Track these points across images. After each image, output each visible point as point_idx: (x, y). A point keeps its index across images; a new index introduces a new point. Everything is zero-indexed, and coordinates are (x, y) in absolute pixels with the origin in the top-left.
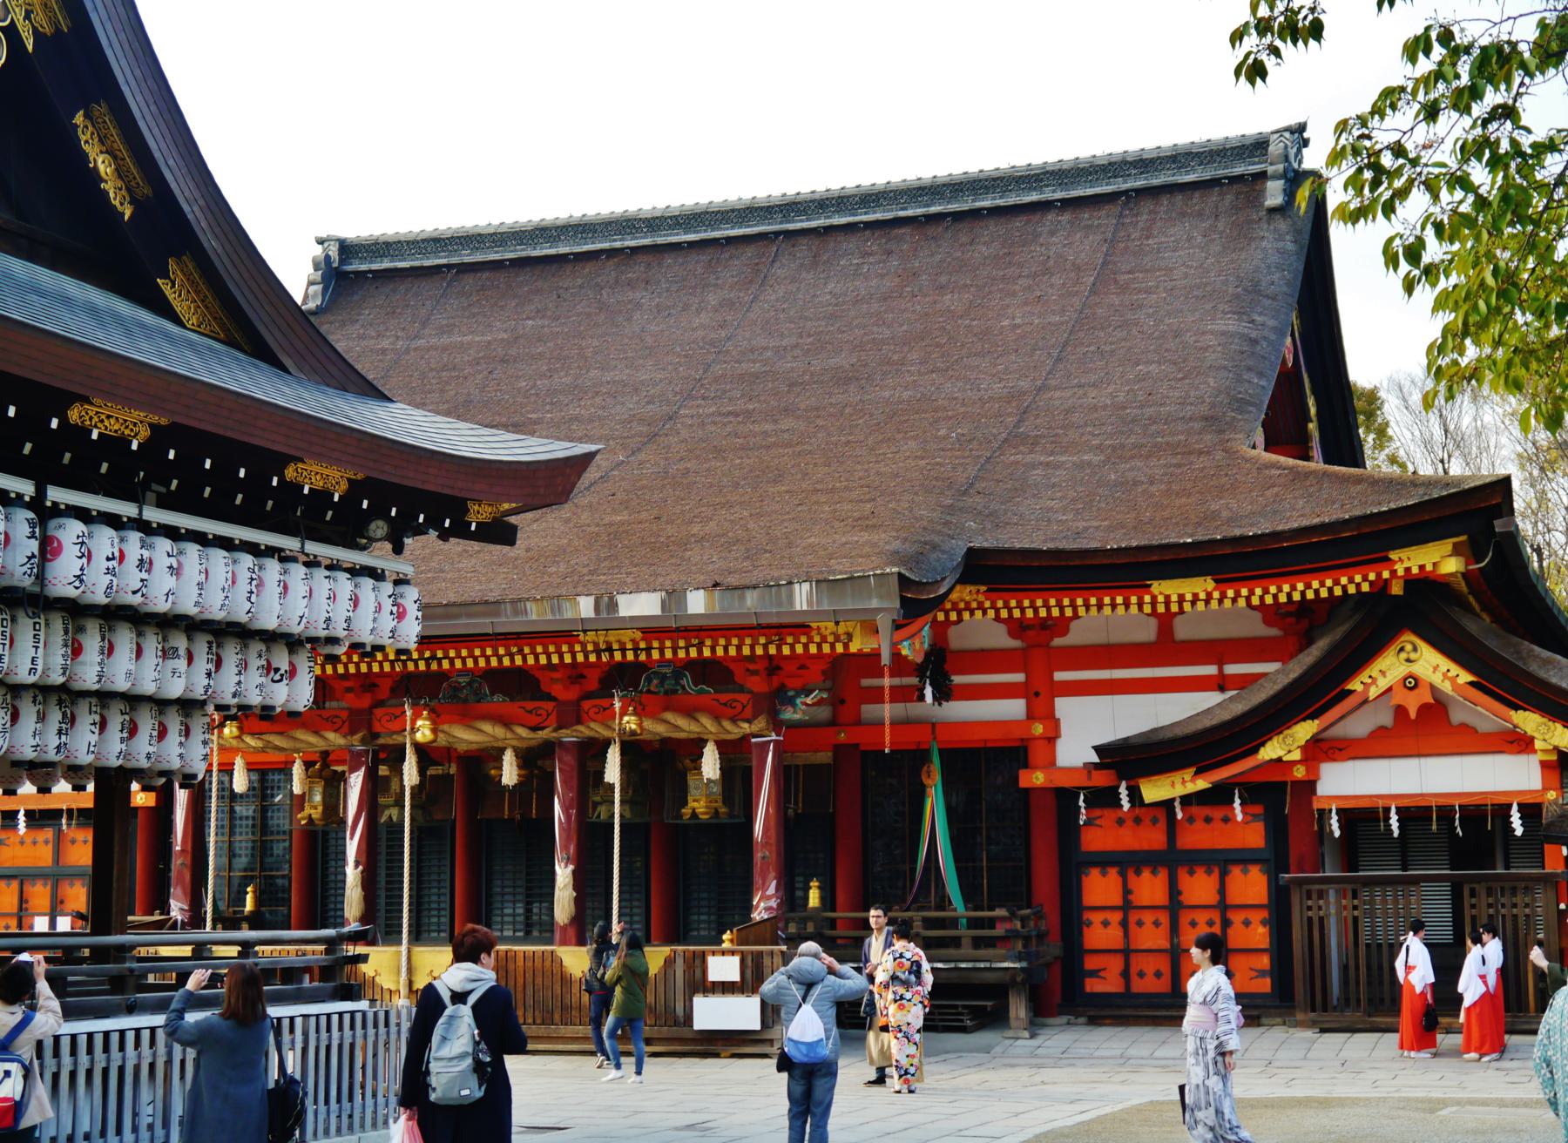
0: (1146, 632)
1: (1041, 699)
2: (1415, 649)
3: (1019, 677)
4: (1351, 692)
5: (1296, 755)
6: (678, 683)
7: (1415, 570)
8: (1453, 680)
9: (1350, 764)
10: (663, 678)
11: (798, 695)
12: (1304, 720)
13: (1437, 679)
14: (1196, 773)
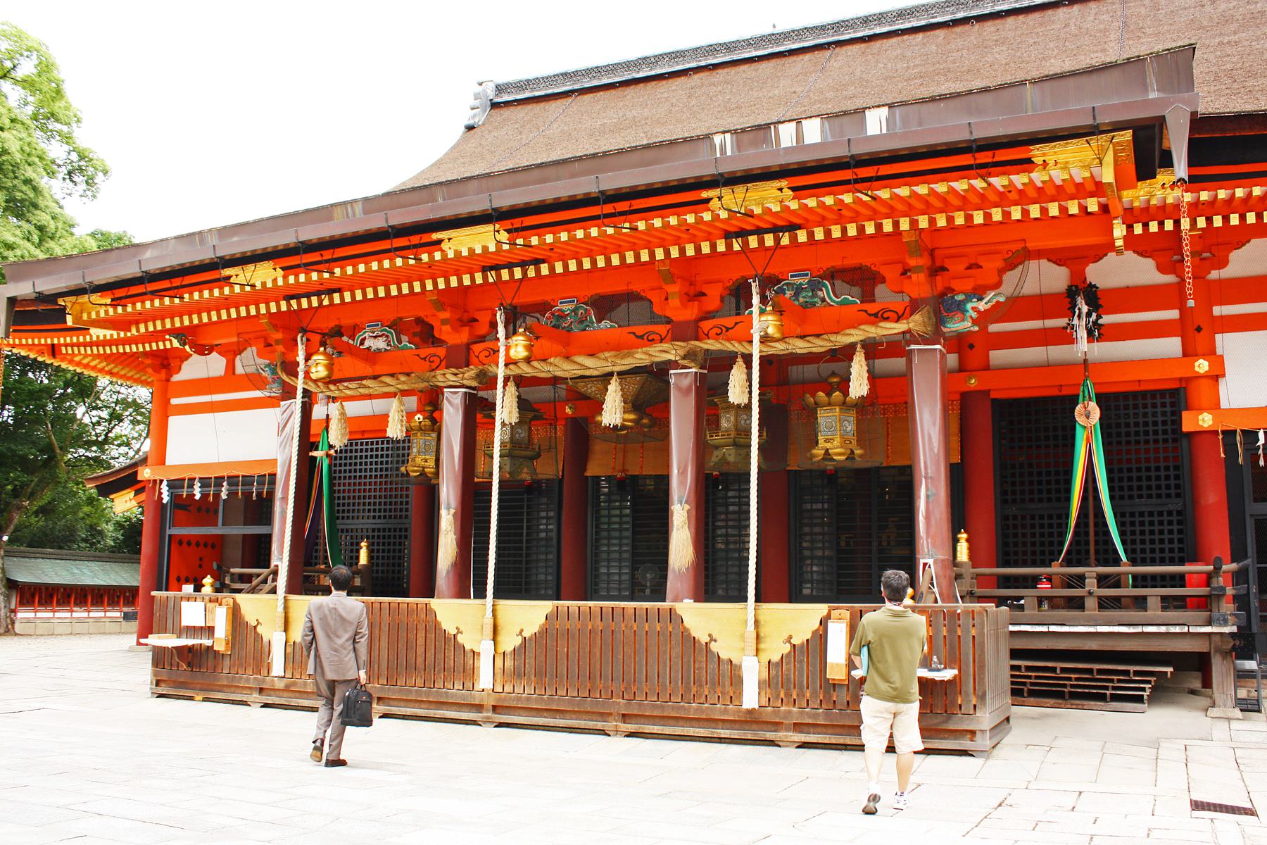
1: (1197, 333)
3: (1173, 314)
6: (814, 296)
10: (798, 290)
11: (968, 299)
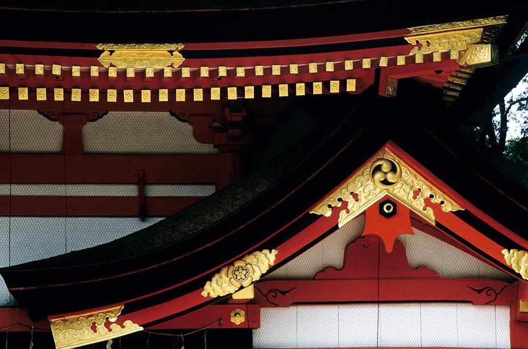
0: (47, 136)
2: (394, 169)
4: (316, 217)
5: (248, 294)
7: (437, 58)
8: (437, 208)
9: (293, 310)
12: (260, 249)
13: (418, 205)
14: (123, 312)
